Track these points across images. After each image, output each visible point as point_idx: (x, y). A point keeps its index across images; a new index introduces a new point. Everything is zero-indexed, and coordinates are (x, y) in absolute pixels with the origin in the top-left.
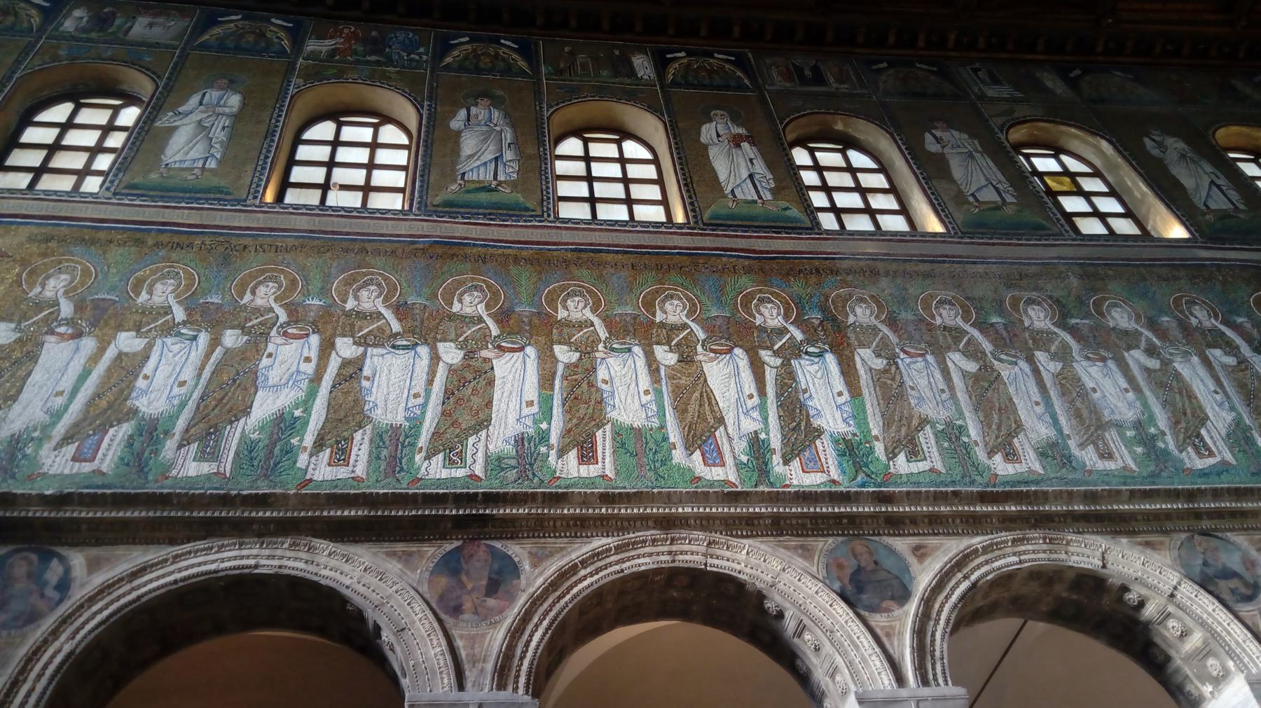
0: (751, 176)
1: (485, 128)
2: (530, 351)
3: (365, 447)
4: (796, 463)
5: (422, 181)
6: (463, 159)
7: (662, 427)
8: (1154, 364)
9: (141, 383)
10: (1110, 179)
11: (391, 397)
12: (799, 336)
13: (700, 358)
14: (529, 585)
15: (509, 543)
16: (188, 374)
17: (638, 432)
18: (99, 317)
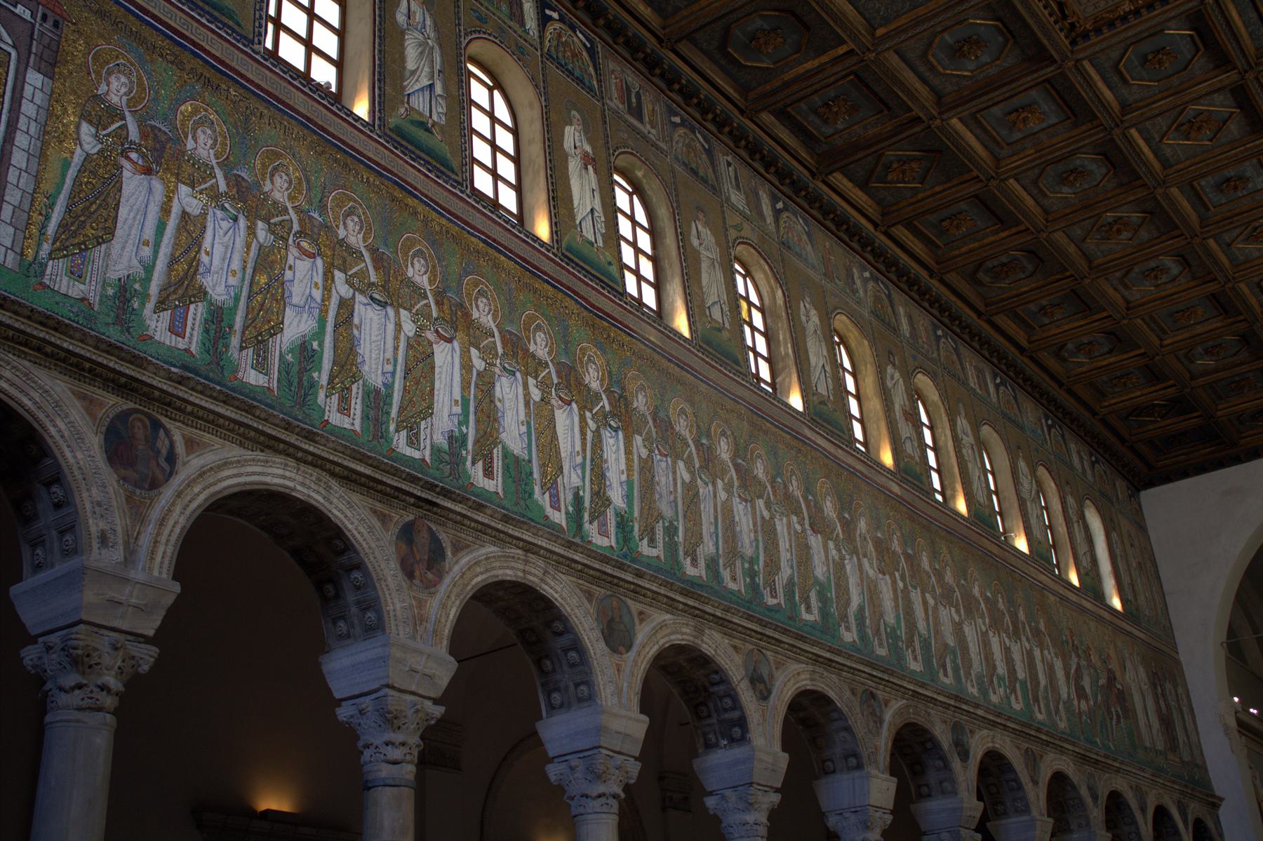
0: (592, 210)
1: (421, 37)
2: (456, 343)
3: (359, 401)
4: (596, 523)
5: (380, 88)
6: (407, 74)
7: (530, 461)
8: (766, 514)
9: (204, 258)
10: (769, 321)
11: (374, 356)
12: (607, 408)
13: (553, 402)
14: (450, 569)
15: (440, 529)
16: (236, 265)
17: (516, 459)
18: (163, 155)
